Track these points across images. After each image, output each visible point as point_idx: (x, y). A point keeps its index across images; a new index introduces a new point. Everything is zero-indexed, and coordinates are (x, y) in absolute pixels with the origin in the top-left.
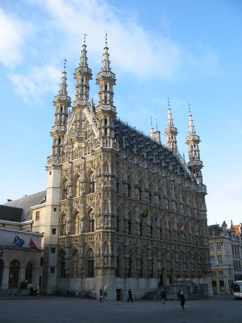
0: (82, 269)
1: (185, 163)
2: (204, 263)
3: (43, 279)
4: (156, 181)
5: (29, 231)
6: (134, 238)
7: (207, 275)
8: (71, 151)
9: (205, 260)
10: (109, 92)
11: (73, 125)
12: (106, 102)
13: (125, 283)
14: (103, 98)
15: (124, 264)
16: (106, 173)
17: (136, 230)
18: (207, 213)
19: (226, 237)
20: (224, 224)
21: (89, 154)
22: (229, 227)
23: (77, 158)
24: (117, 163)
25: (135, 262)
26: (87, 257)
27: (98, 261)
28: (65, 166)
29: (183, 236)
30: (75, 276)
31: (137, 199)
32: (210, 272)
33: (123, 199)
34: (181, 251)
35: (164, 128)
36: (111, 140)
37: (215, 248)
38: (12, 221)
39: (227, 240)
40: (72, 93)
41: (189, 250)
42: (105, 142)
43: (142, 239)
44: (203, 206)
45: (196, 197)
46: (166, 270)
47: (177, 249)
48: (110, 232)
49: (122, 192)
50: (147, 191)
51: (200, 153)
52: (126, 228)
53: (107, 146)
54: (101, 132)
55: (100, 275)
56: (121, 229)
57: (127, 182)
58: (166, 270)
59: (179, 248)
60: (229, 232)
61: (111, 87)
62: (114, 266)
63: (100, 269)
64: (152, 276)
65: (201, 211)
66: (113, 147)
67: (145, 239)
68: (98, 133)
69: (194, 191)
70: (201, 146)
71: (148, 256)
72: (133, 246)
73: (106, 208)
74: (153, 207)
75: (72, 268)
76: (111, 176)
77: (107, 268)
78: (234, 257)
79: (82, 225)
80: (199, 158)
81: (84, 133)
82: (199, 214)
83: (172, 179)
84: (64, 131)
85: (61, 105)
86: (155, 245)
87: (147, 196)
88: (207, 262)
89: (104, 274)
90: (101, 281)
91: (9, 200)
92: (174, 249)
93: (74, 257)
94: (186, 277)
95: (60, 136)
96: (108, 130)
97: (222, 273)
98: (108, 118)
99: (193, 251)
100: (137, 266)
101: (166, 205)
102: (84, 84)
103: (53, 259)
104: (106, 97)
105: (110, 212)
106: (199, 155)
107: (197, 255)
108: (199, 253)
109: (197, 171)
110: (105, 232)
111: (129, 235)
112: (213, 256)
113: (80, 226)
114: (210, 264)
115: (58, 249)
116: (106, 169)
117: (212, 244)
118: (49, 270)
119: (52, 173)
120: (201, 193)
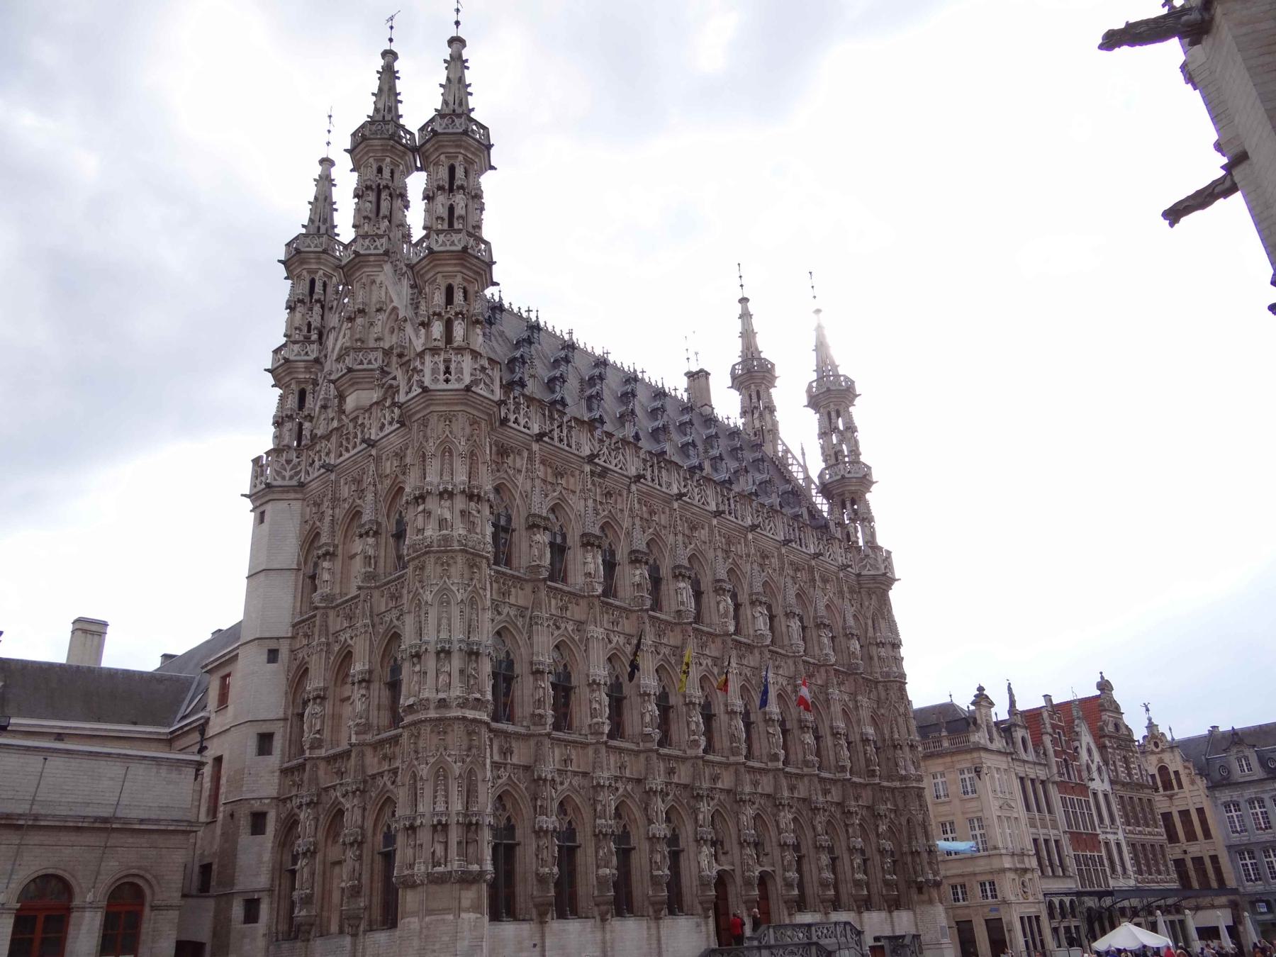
0: (356, 892)
1: (807, 478)
2: (905, 848)
4: (683, 527)
6: (585, 745)
7: (925, 897)
8: (335, 424)
10: (461, 187)
12: (451, 224)
15: (537, 861)
17: (592, 708)
18: (903, 651)
19: (994, 747)
20: (982, 699)
21: (391, 423)
22: (1000, 712)
23: (354, 447)
24: (503, 451)
25: (591, 850)
26: (380, 837)
27: (410, 852)
28: (314, 485)
29: (809, 738)
30: (334, 928)
31: (593, 589)
32: (937, 884)
33: (528, 588)
34: (804, 800)
37: (956, 789)
38: (135, 723)
39: (994, 757)
41: (835, 795)
42: (442, 367)
43: (621, 750)
44: (883, 625)
45: (852, 591)
46: (739, 880)
47: (786, 794)
48: (457, 718)
49: (524, 563)
51: (860, 436)
52: (540, 703)
54: (428, 335)
55: (413, 914)
56: (524, 708)
58: (739, 880)
59: (792, 788)
60: (1006, 729)
62: (475, 867)
63: (414, 886)
64: (675, 905)
65: (877, 645)
66: (475, 382)
67: (637, 753)
68: (422, 340)
69: (844, 567)
70: (858, 412)
71: (650, 822)
72: (576, 781)
73: (444, 621)
74: (667, 623)
75: (326, 894)
76: (463, 492)
77: (440, 880)
81: (380, 355)
82: (871, 658)
83: (749, 522)
84: (317, 361)
86: (683, 774)
87: (637, 578)
88: (920, 844)
90: (416, 943)
93: (335, 842)
94: (836, 905)
95: (306, 381)
96: (459, 330)
97: (993, 890)
98: (457, 282)
99: (857, 799)
100: (598, 867)
101: (726, 615)
103: (256, 861)
104: (451, 209)
106: (856, 442)
108: (882, 808)
109: (853, 502)
111: (556, 734)
112: (952, 823)
113: (354, 709)
114: (931, 851)
117: (943, 775)
118: (238, 911)
120: (874, 577)
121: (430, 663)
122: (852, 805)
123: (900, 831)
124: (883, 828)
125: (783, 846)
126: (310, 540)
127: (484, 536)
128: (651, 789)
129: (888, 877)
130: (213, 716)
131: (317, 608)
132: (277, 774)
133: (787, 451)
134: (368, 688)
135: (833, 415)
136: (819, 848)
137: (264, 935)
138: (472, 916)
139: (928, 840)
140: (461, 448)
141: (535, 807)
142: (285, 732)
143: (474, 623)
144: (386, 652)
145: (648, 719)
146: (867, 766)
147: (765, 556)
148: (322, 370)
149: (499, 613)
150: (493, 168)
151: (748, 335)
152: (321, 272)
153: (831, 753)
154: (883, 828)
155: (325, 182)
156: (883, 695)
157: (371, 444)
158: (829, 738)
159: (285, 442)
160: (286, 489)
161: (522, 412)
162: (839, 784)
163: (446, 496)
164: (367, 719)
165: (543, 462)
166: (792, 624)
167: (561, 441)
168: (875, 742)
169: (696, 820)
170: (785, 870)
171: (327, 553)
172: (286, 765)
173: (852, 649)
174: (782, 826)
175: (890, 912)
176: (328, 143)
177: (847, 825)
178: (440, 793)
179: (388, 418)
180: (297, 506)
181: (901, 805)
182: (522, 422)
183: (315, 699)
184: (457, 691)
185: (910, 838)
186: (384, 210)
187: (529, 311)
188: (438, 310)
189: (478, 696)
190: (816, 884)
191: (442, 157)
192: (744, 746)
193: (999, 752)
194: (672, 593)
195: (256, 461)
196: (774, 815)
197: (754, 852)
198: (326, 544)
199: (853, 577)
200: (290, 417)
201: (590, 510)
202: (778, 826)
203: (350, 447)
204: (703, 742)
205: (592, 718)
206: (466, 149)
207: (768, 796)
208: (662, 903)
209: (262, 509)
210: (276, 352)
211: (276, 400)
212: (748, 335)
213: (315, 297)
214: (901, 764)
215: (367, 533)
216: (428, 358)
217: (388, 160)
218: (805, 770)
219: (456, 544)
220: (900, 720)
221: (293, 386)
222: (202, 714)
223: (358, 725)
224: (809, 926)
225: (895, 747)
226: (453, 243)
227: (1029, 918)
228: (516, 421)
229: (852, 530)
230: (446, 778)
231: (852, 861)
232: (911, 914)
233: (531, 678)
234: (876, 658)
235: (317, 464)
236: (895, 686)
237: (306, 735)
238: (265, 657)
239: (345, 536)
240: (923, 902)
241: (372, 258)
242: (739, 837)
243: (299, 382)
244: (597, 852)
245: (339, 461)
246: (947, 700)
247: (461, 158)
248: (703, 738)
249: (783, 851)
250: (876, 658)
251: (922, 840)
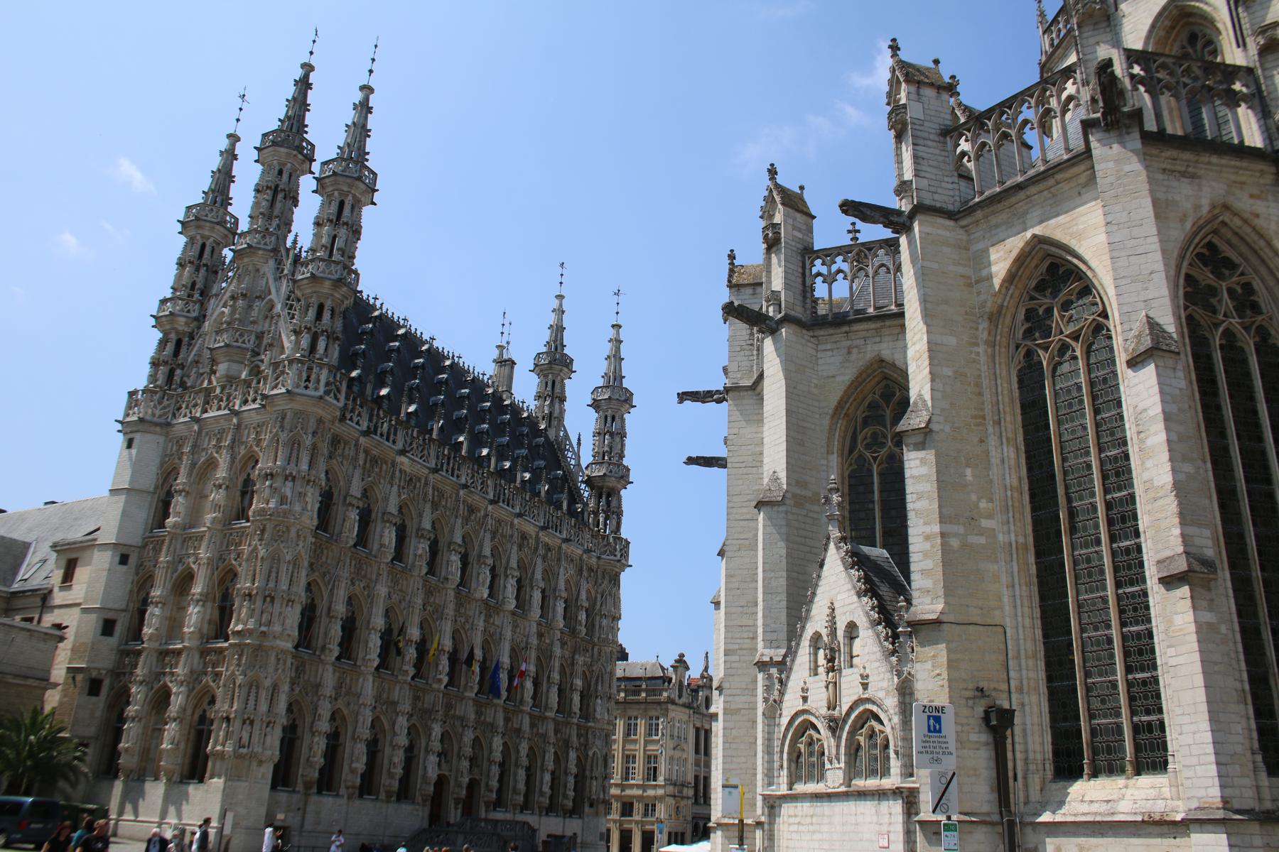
1: (579, 465)
2: (588, 773)
5: (31, 620)
10: (346, 224)
11: (225, 306)
13: (303, 810)
14: (324, 240)
16: (291, 469)
20: (681, 663)
21: (254, 401)
23: (219, 409)
35: (528, 348)
36: (325, 373)
40: (242, 203)
42: (304, 375)
51: (627, 441)
54: (297, 342)
61: (357, 207)
66: (327, 393)
69: (588, 551)
70: (632, 421)
73: (273, 575)
78: (697, 764)
79: (194, 617)
80: (621, 456)
81: (253, 338)
82: (593, 626)
84: (196, 319)
85: (203, 236)
95: (184, 333)
96: (321, 345)
102: (282, 186)
105: (285, 588)
106: (623, 445)
112: (634, 757)
115: (112, 688)
116: (294, 455)
119: (135, 444)
121: (259, 602)
126: (168, 473)
133: (567, 436)
135: (609, 419)
140: (308, 443)
144: (222, 581)
148: (199, 328)
151: (558, 330)
155: (230, 155)
160: (156, 424)
167: (382, 435)
171: (183, 490)
176: (238, 120)
178: (252, 699)
180: (162, 439)
182: (355, 419)
186: (276, 212)
187: (376, 299)
191: (336, 193)
193: (684, 705)
195: (132, 394)
199: (594, 560)
200: (166, 363)
204: (446, 680)
209: (131, 436)
210: (164, 301)
211: (156, 343)
212: (558, 330)
213: (204, 261)
215: (220, 486)
216: (295, 366)
224: (497, 821)
226: (330, 273)
227: (676, 834)
229: (601, 520)
230: (258, 687)
232: (580, 821)
238: (117, 559)
243: (177, 333)
246: (654, 660)
247: (350, 197)
251: (601, 768)
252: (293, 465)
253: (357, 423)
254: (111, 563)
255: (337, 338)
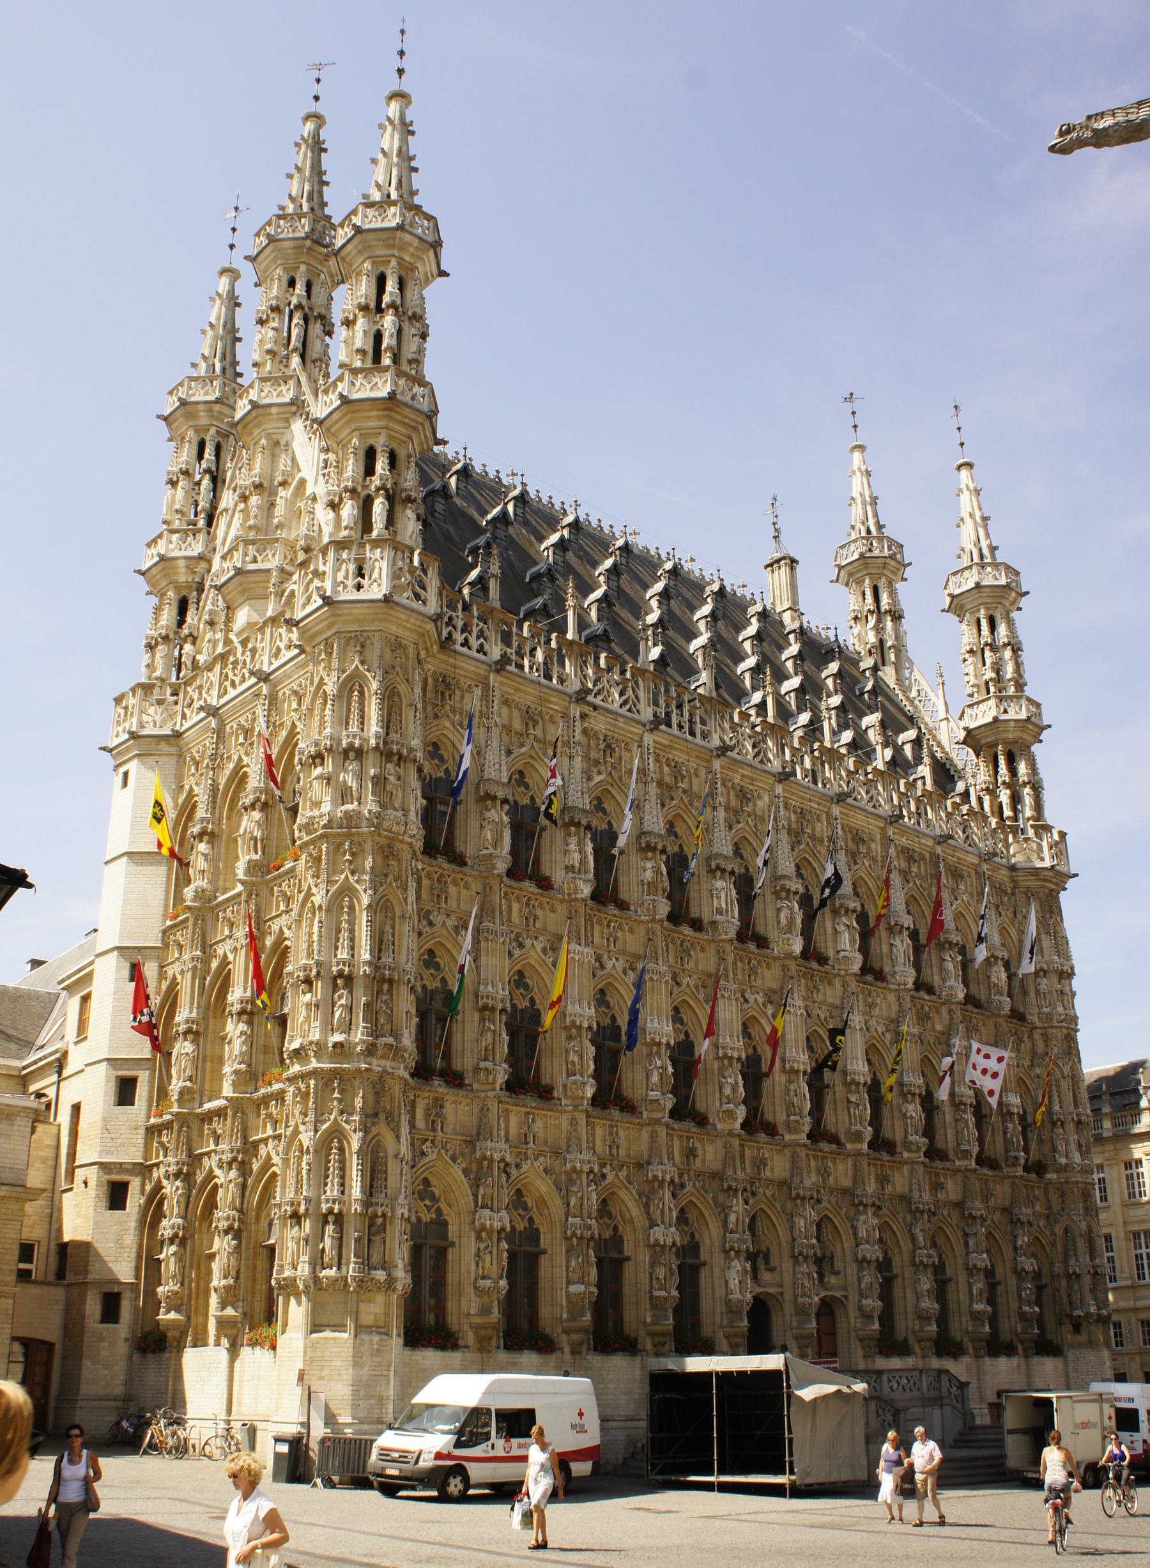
2: (1058, 1268)
3: (64, 1358)
7: (1082, 1338)
8: (220, 649)
9: (1069, 1251)
12: (377, 358)
18: (1076, 983)
21: (289, 647)
23: (243, 680)
25: (560, 1259)
46: (788, 1308)
47: (871, 1187)
50: (650, 848)
53: (359, 587)
54: (338, 519)
57: (500, 794)
58: (788, 1308)
71: (653, 1224)
84: (201, 557)
87: (649, 875)
88: (1081, 1263)
89: (316, 1327)
91: (36, 963)
92: (846, 1182)
95: (189, 588)
98: (380, 443)
100: (568, 1283)
104: (378, 337)
107: (1016, 1222)
108: (1024, 1212)
110: (335, 1073)
114: (1096, 1274)
118: (93, 1307)
122: (977, 1207)
123: (1053, 1244)
124: (1023, 1240)
125: (862, 1262)
127: (405, 811)
128: (655, 1177)
129: (1026, 1308)
130: (72, 1050)
131: (189, 908)
132: (142, 1131)
134: (250, 1023)
136: (918, 1266)
137: (126, 1340)
138: (376, 1338)
139: (1092, 1258)
141: (476, 1196)
142: (152, 1076)
143: (388, 938)
145: (655, 1078)
146: (1007, 1151)
147: (858, 838)
149: (431, 924)
150: (443, 274)
152: (213, 431)
153: (950, 1132)
154: (1023, 1240)
156: (1040, 1045)
157: (265, 678)
158: (947, 1109)
159: (158, 673)
161: (475, 631)
162: (959, 1177)
163: (352, 755)
164: (249, 1065)
165: (506, 702)
166: (897, 942)
168: (1023, 1118)
169: (725, 1222)
170: (862, 1295)
172: (153, 1121)
173: (994, 979)
174: (862, 1233)
175: (1026, 1357)
177: (966, 1235)
179: (285, 641)
181: (1056, 1207)
182: (475, 643)
183: (185, 1033)
184: (359, 1035)
185: (1066, 1255)
188: (350, 484)
189: (390, 1040)
190: (910, 1317)
192: (808, 1120)
194: (705, 894)
196: (852, 1220)
197: (814, 1268)
198: (203, 820)
199: (1005, 872)
201: (578, 774)
202: (855, 1234)
203: (237, 680)
205: (568, 1075)
206: (401, 249)
207: (845, 1191)
208: (663, 1334)
214: (1061, 1147)
217: (303, 268)
218: (906, 1155)
219: (364, 823)
220: (1065, 1085)
221: (170, 594)
222: (58, 1046)
223: (236, 1072)
225: (1054, 1124)
228: (466, 643)
231: (970, 1285)
233: (477, 1016)
234: (1033, 994)
235: (196, 705)
236: (1059, 1034)
237: (174, 1081)
239: (230, 809)
240: (1079, 1346)
241: (274, 410)
242: (793, 1247)
244: (568, 1261)
245: (222, 701)
247: (394, 263)
248: (743, 1107)
249: (860, 1269)
250: (1033, 994)
252: (354, 728)
253: (481, 650)
254: (117, 980)
255: (409, 500)
